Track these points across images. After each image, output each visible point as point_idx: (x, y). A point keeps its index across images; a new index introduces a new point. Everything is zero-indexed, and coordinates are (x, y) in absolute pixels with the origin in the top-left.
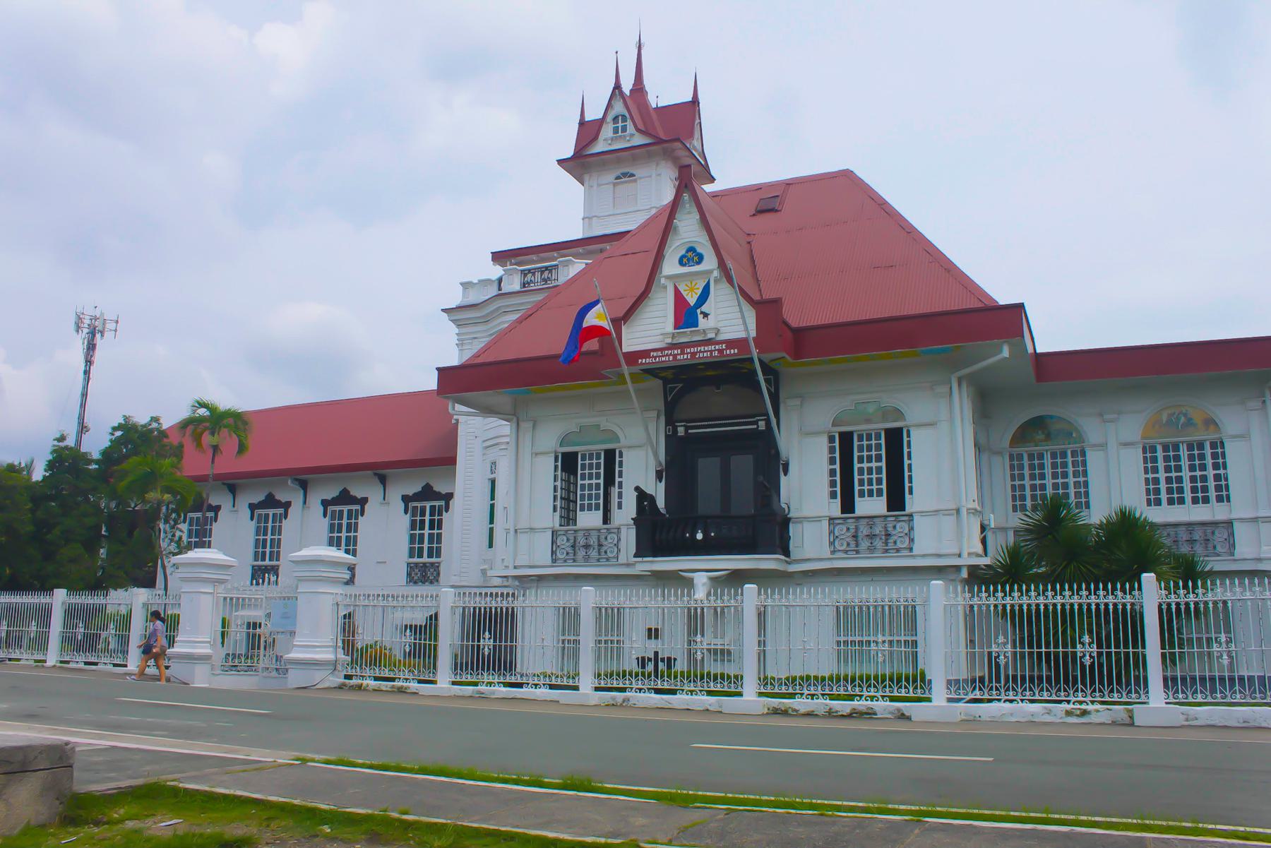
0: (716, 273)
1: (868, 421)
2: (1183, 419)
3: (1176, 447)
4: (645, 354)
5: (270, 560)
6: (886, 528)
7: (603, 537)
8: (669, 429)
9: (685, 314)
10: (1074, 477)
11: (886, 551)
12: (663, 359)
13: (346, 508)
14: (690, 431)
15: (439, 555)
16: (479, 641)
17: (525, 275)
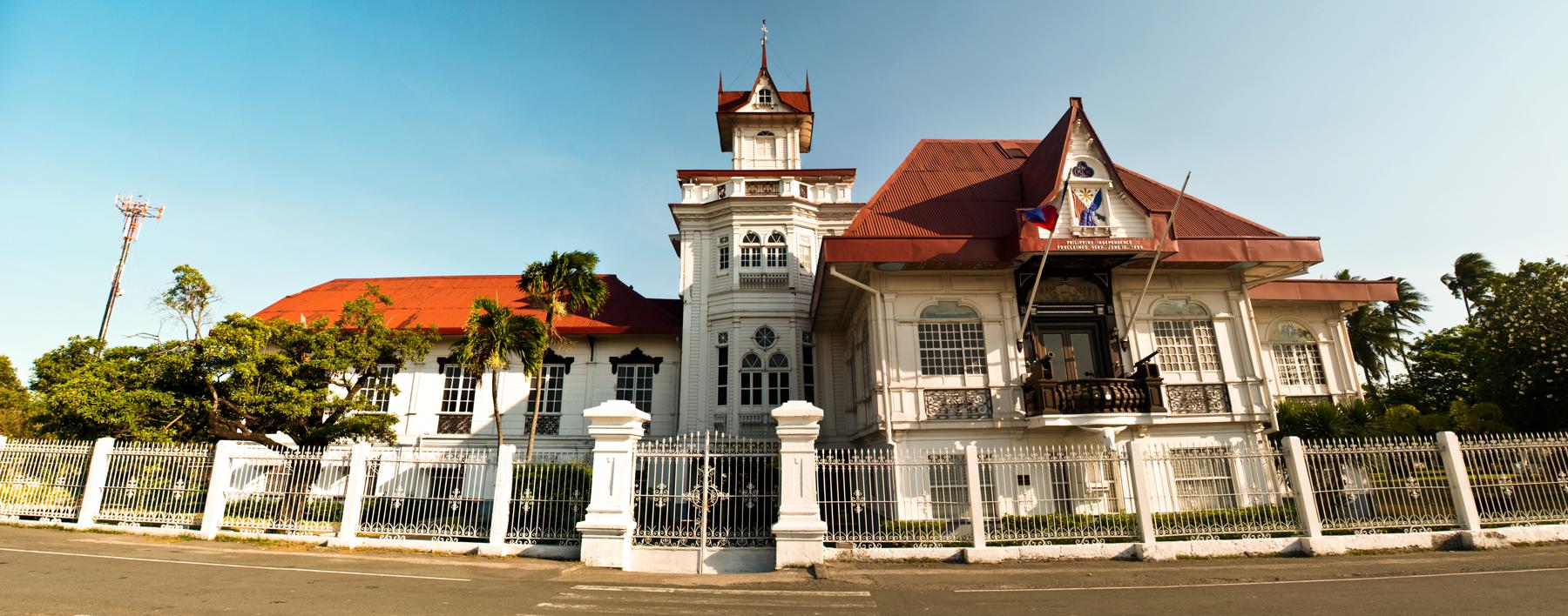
0: (1111, 185)
5: (460, 411)
12: (1080, 247)
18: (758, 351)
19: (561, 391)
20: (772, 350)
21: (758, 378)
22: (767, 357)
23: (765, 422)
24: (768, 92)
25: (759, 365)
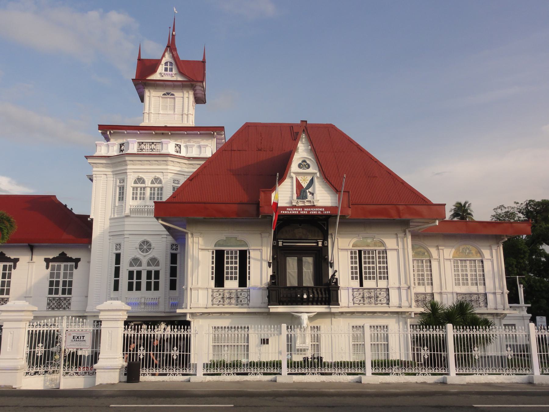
0: (318, 174)
1: (368, 246)
8: (275, 242)
9: (301, 192)
12: (294, 212)
14: (284, 244)
15: (70, 292)
19: (10, 281)
21: (139, 273)
22: (146, 260)
24: (171, 63)
25: (140, 265)
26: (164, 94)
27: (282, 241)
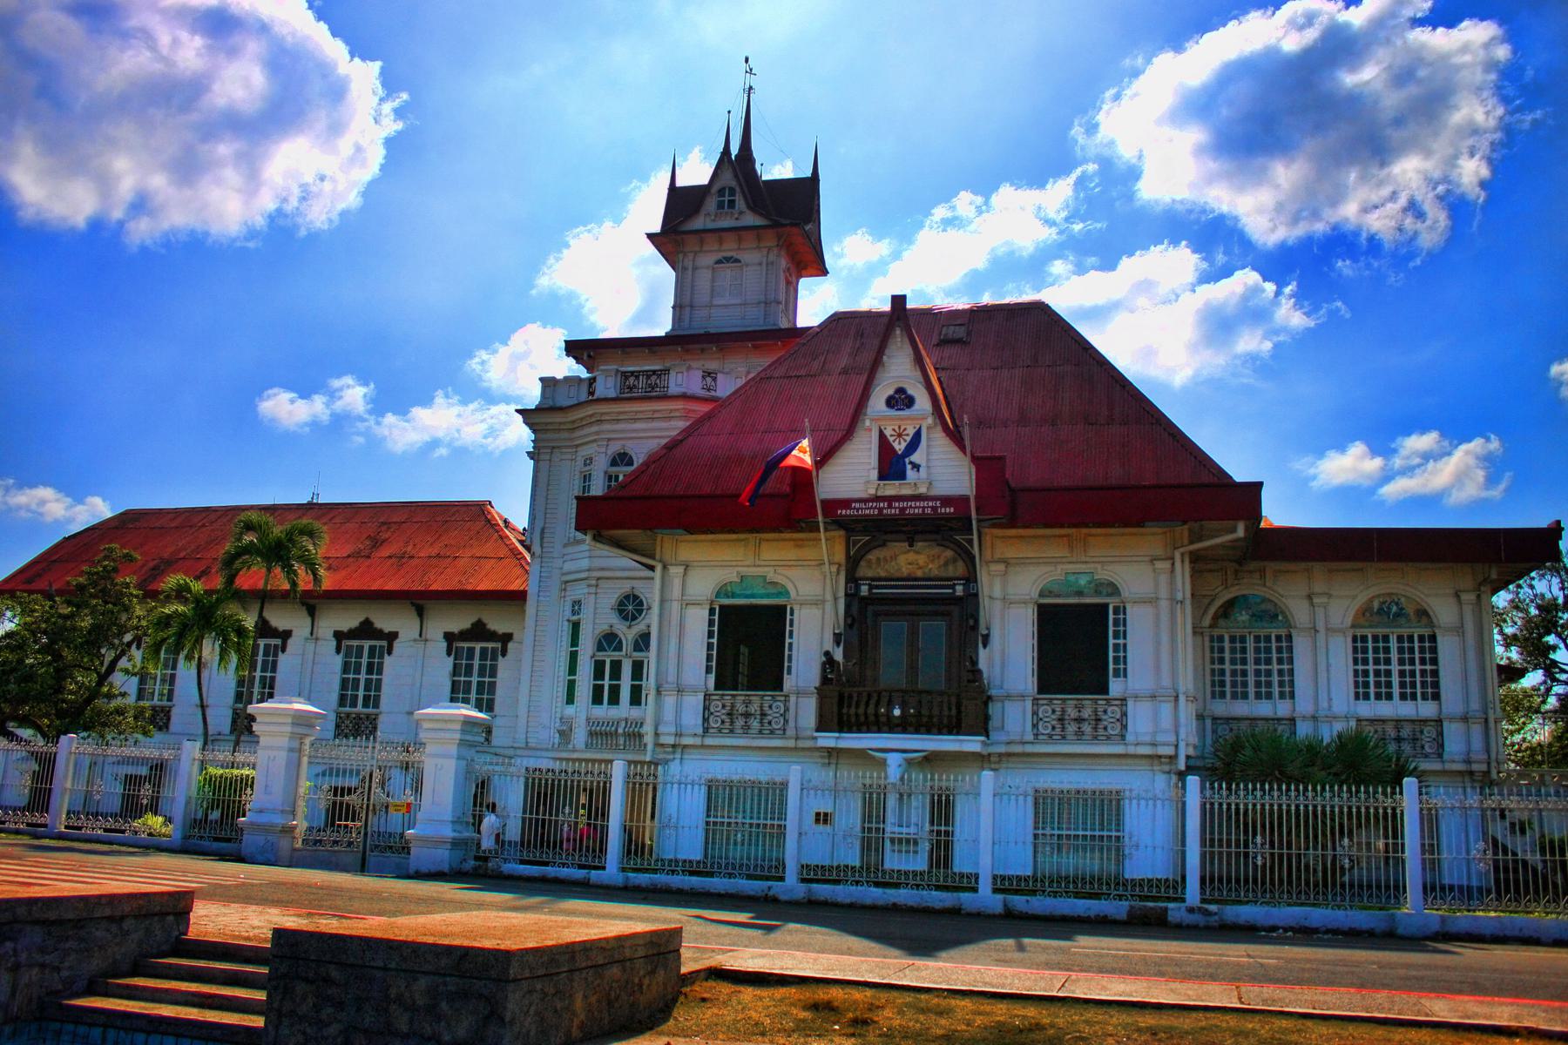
0: (930, 421)
2: (1394, 609)
3: (1386, 638)
4: (846, 503)
6: (1096, 711)
7: (767, 705)
9: (891, 464)
10: (1278, 664)
11: (1095, 738)
12: (867, 512)
13: (367, 644)
14: (874, 591)
16: (557, 815)
17: (627, 378)
18: (621, 628)
19: (381, 680)
20: (639, 627)
21: (616, 667)
23: (620, 731)
25: (619, 648)
26: (719, 262)
27: (869, 585)
